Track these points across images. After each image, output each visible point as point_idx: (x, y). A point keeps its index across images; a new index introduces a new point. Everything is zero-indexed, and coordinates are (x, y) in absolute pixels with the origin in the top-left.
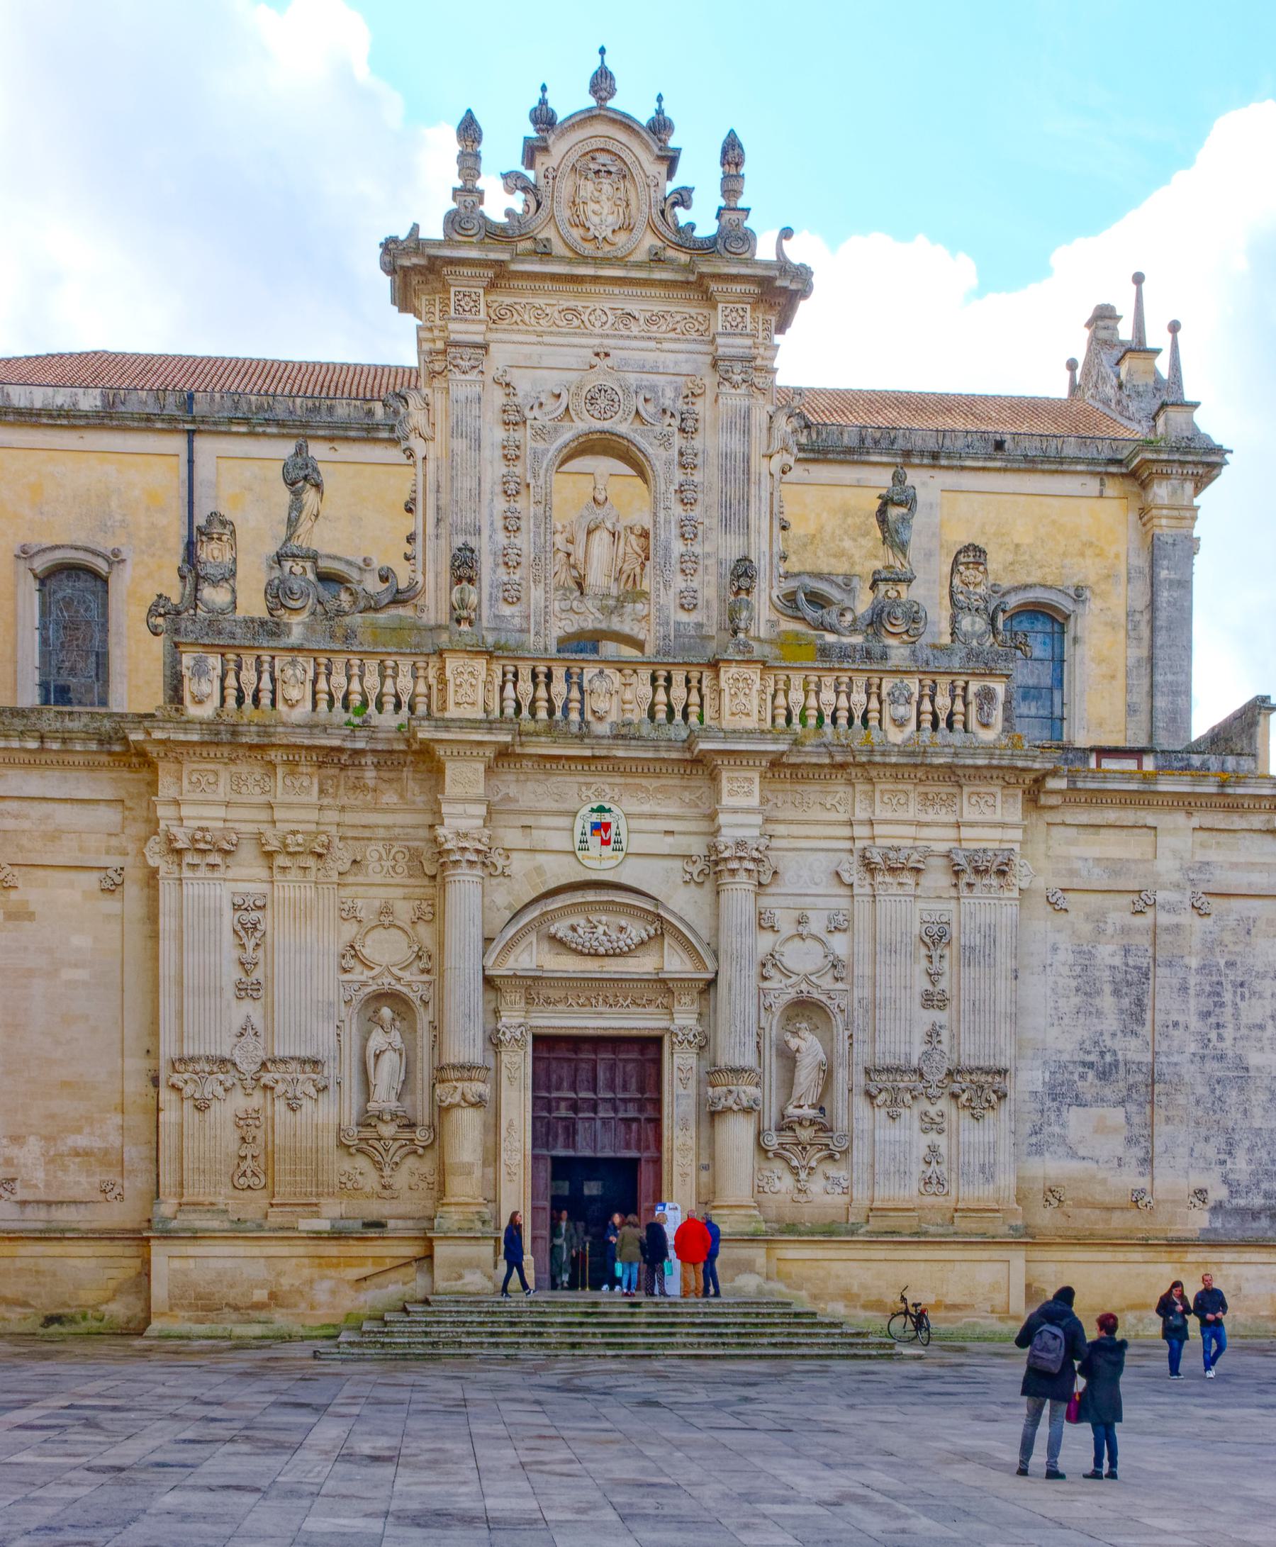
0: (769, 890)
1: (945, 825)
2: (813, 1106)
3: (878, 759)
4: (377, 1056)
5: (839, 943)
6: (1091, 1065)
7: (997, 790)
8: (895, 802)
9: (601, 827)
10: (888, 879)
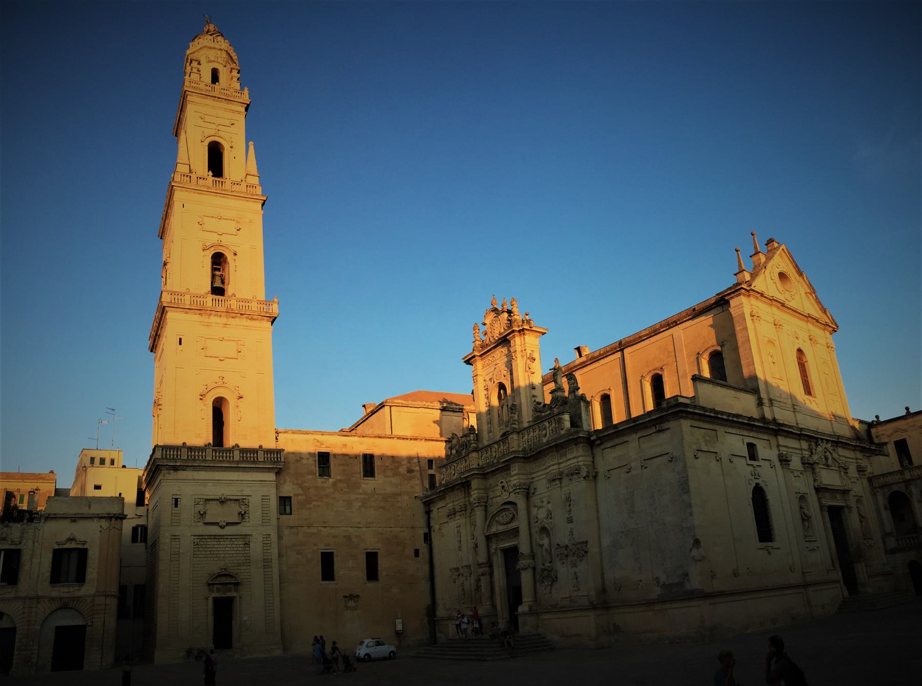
0: (536, 494)
1: (564, 462)
7: (574, 446)
9: (503, 487)
10: (554, 483)
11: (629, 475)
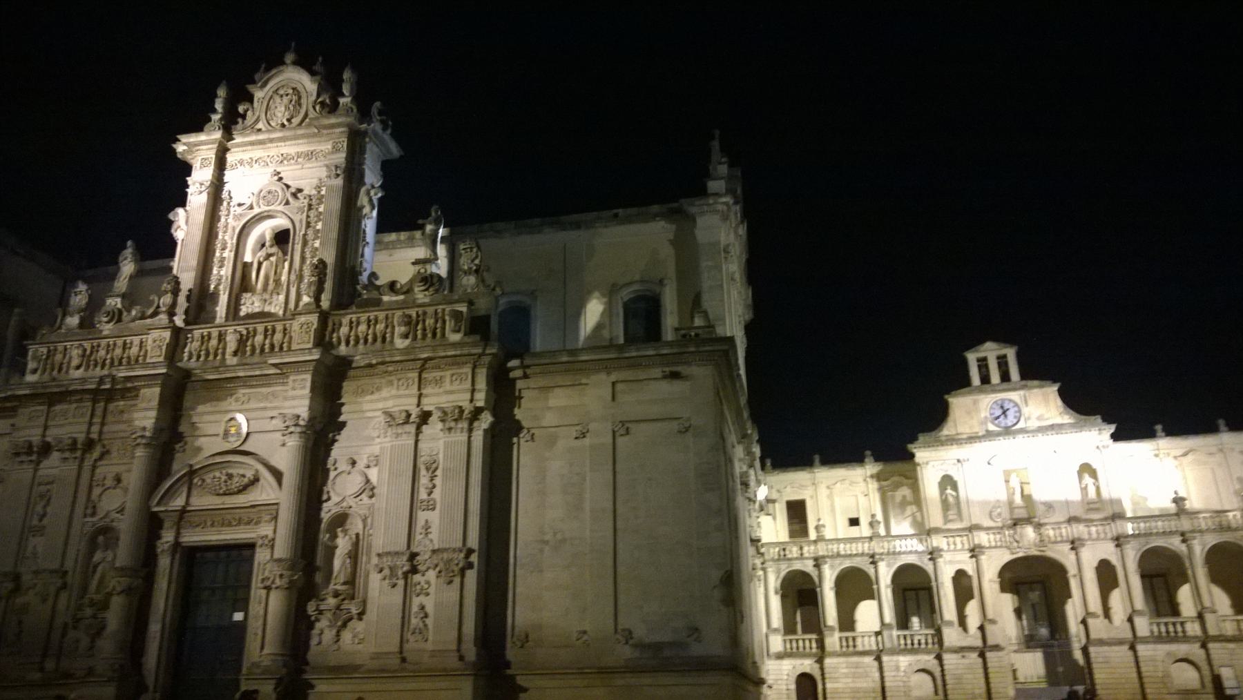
2: (344, 583)
3: (388, 359)
4: (96, 567)
5: (373, 474)
6: (546, 543)
8: (406, 385)
11: (578, 442)
